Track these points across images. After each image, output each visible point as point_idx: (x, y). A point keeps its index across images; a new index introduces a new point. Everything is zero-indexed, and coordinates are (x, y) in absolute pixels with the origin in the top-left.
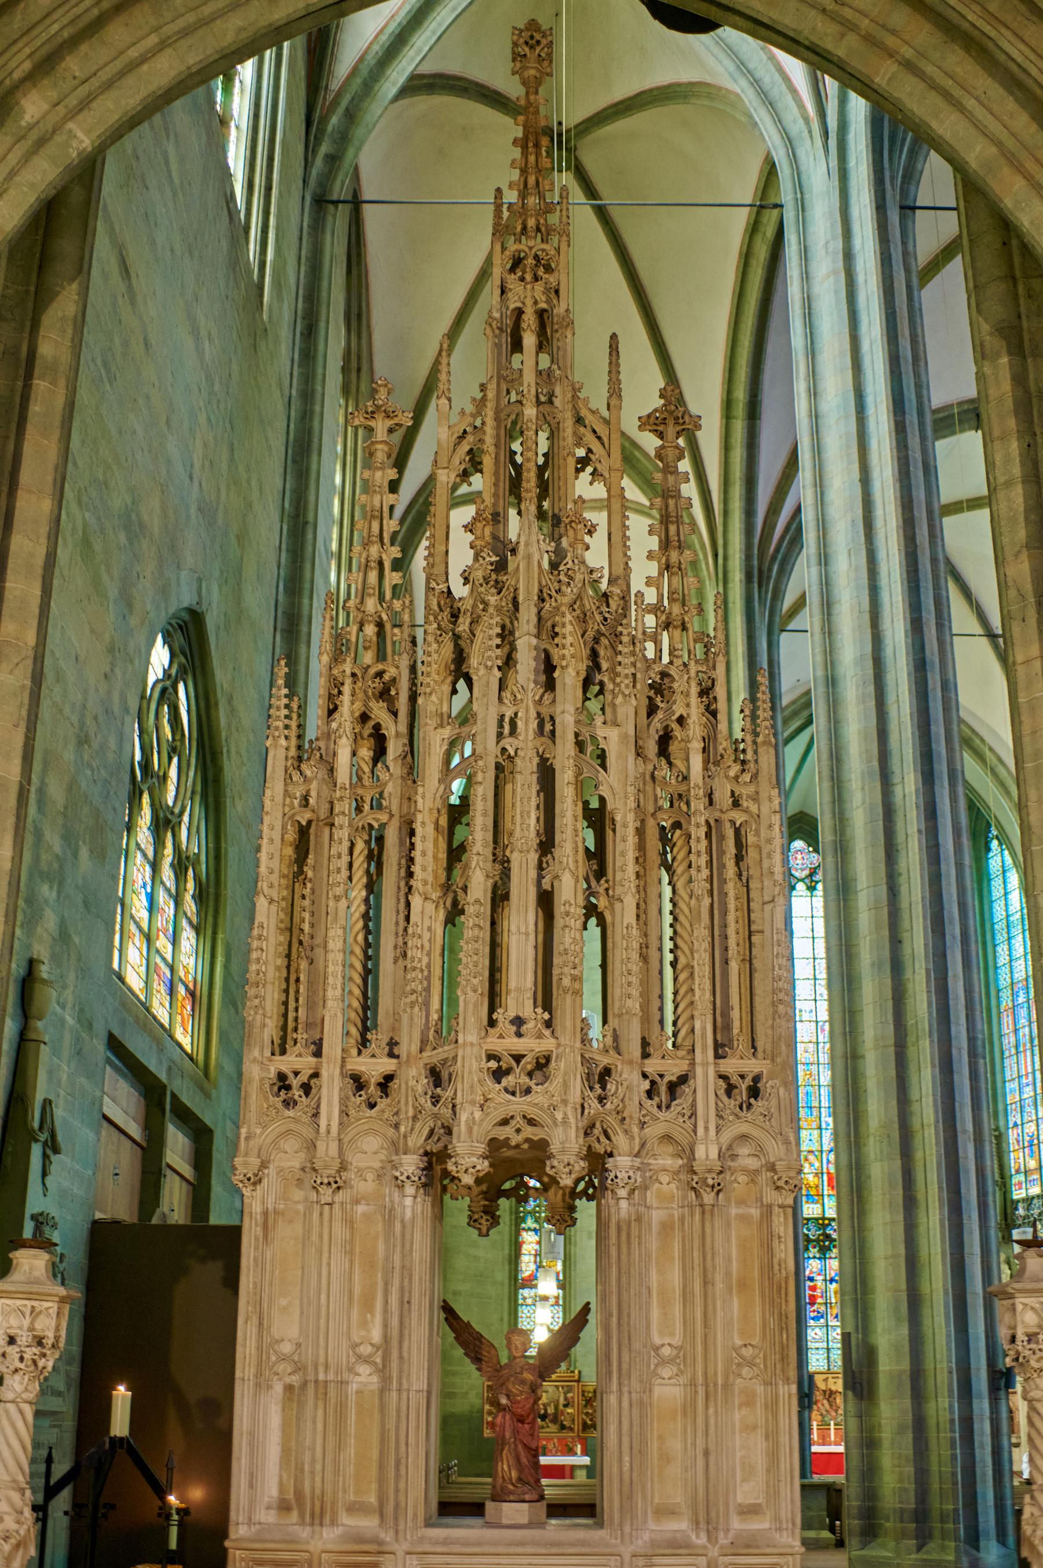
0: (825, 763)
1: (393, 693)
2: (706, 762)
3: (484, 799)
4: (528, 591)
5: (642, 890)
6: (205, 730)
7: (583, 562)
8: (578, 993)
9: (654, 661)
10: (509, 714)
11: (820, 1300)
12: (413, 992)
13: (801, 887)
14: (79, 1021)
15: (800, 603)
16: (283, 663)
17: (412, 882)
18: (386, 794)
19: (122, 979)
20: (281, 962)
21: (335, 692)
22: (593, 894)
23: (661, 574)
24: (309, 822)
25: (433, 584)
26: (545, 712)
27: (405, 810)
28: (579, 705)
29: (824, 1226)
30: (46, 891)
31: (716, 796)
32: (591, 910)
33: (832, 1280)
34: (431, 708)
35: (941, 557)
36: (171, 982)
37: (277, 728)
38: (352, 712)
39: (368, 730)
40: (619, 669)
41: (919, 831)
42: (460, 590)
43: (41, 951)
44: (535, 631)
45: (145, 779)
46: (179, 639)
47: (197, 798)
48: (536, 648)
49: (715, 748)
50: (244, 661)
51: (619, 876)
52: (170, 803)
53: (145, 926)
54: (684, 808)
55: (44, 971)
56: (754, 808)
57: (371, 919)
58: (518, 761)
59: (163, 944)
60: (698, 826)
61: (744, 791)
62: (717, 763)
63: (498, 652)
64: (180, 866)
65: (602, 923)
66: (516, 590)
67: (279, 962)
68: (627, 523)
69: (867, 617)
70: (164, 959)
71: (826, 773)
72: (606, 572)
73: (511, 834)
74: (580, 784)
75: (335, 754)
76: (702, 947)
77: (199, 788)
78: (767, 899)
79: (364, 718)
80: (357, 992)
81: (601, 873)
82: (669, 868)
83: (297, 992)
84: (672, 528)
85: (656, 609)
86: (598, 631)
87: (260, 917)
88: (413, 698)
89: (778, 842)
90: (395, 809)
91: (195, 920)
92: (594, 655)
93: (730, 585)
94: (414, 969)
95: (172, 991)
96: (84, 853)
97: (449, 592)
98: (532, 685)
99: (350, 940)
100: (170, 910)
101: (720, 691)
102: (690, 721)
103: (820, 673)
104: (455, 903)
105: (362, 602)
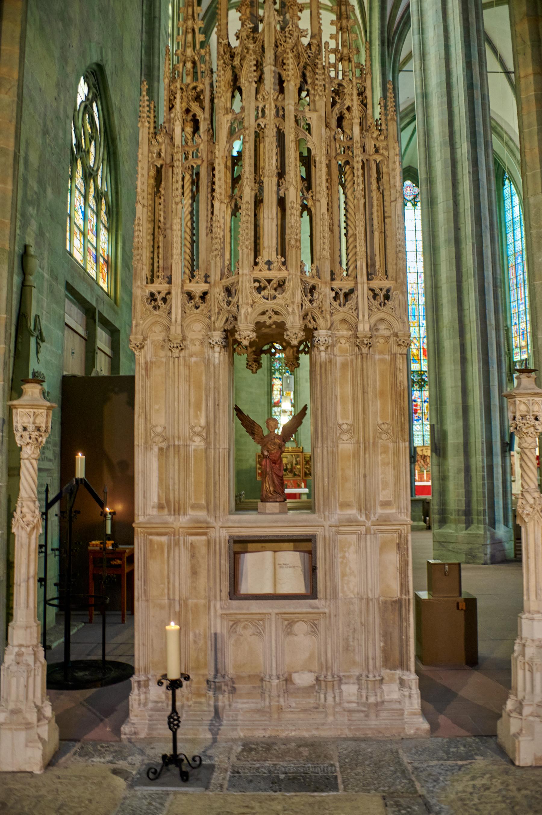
1: (202, 97)
2: (361, 130)
3: (250, 150)
4: (270, 42)
5: (330, 195)
7: (297, 27)
8: (299, 248)
9: (335, 78)
10: (261, 106)
11: (419, 411)
12: (216, 249)
16: (145, 83)
17: (214, 194)
18: (200, 150)
20: (150, 237)
21: (172, 98)
22: (306, 199)
23: (338, 32)
24: (162, 166)
25: (221, 40)
26: (279, 104)
27: (210, 157)
28: (297, 101)
29: (421, 375)
31: (367, 147)
32: (304, 207)
33: (425, 402)
34: (221, 104)
37: (143, 117)
38: (181, 108)
39: (189, 118)
40: (317, 82)
42: (235, 43)
44: (273, 63)
48: (274, 72)
49: (366, 123)
54: (351, 154)
56: (386, 154)
57: (194, 215)
58: (266, 131)
60: (358, 162)
61: (381, 145)
62: (367, 131)
63: (255, 74)
65: (310, 214)
66: (263, 41)
67: (149, 237)
72: (309, 31)
73: (263, 169)
78: (393, 199)
79: (188, 111)
80: (188, 251)
81: (309, 188)
82: (343, 186)
83: (158, 253)
84: (343, 8)
85: (335, 51)
86: (306, 63)
87: (139, 214)
88: (212, 100)
90: (204, 157)
92: (304, 76)
94: (216, 238)
97: (229, 44)
98: (272, 91)
99: (184, 225)
101: (368, 93)
102: (353, 109)
104: (236, 205)
105: (185, 51)
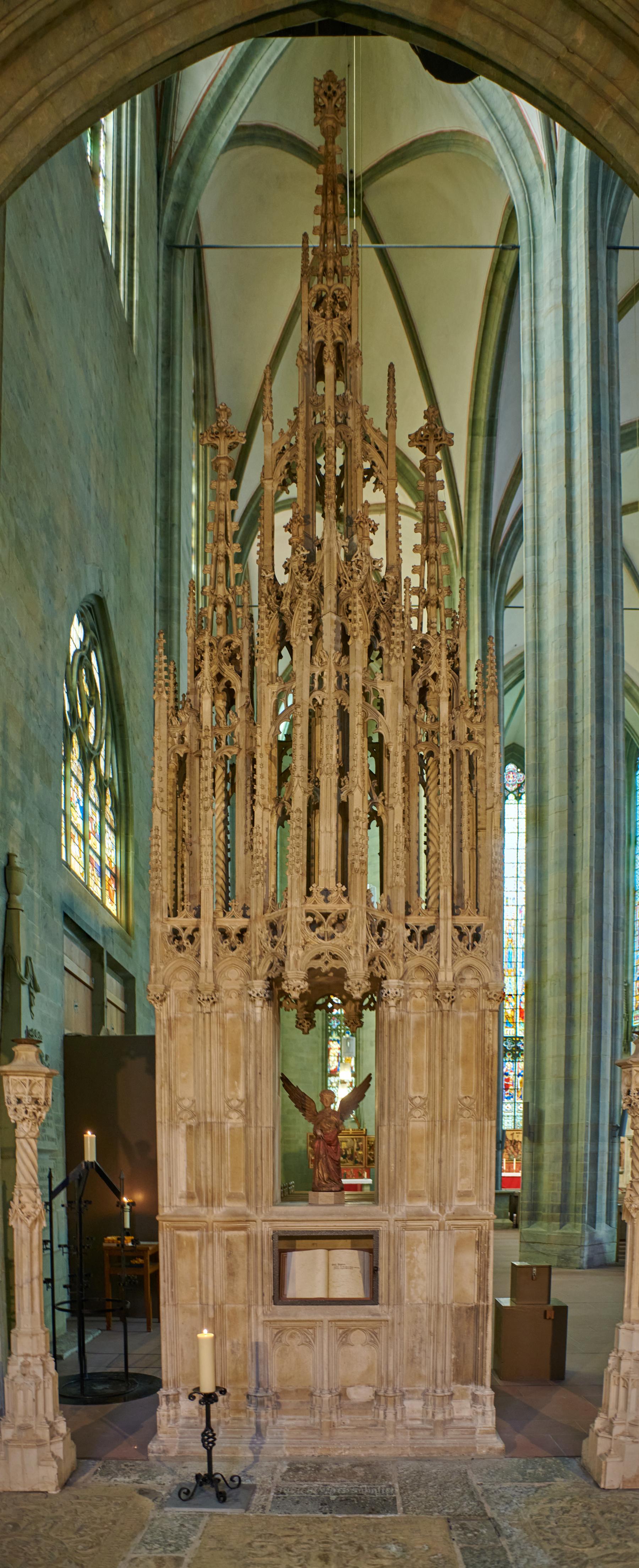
0: (531, 707)
1: (238, 658)
2: (451, 707)
3: (302, 737)
4: (330, 579)
5: (407, 800)
6: (111, 687)
7: (368, 555)
8: (365, 873)
9: (417, 632)
10: (318, 673)
12: (258, 873)
13: (511, 797)
14: (43, 896)
15: (519, 585)
16: (162, 636)
17: (255, 797)
18: (236, 734)
19: (68, 867)
20: (171, 853)
21: (199, 657)
22: (375, 804)
23: (423, 564)
24: (185, 755)
25: (264, 574)
26: (342, 671)
27: (249, 746)
28: (365, 665)
30: (14, 806)
31: (457, 732)
32: (373, 815)
34: (265, 669)
35: (619, 547)
36: (101, 868)
37: (160, 686)
38: (211, 673)
39: (222, 687)
40: (393, 638)
41: (592, 757)
42: (283, 578)
43: (14, 848)
44: (334, 609)
45: (74, 725)
46: (89, 617)
47: (110, 738)
48: (336, 623)
49: (458, 697)
50: (135, 635)
51: (391, 791)
52: (92, 742)
53: (81, 829)
54: (436, 741)
55: (18, 862)
56: (482, 741)
57: (228, 822)
58: (324, 708)
59: (93, 842)
60: (444, 754)
61: (476, 728)
62: (458, 708)
63: (310, 625)
64: (102, 786)
65: (380, 824)
66: (322, 577)
67: (170, 853)
68: (400, 523)
69: (565, 595)
70: (95, 853)
71: (531, 715)
72: (384, 562)
73: (320, 762)
74: (365, 725)
75: (200, 705)
76: (446, 840)
77: (110, 730)
78: (489, 806)
79: (219, 677)
80: (221, 873)
81: (379, 789)
82: (425, 785)
83: (183, 874)
84: (431, 526)
85: (419, 591)
86: (379, 609)
87: (156, 823)
88: (252, 662)
89: (497, 766)
90: (242, 744)
91: (113, 825)
92: (376, 627)
93: (471, 572)
94: (258, 857)
95: (101, 875)
96: (37, 778)
97: (275, 579)
98: (333, 651)
99: (215, 838)
100: (96, 818)
101: (462, 654)
102: (441, 677)
103: (531, 639)
104: (284, 811)
105: (214, 588)
